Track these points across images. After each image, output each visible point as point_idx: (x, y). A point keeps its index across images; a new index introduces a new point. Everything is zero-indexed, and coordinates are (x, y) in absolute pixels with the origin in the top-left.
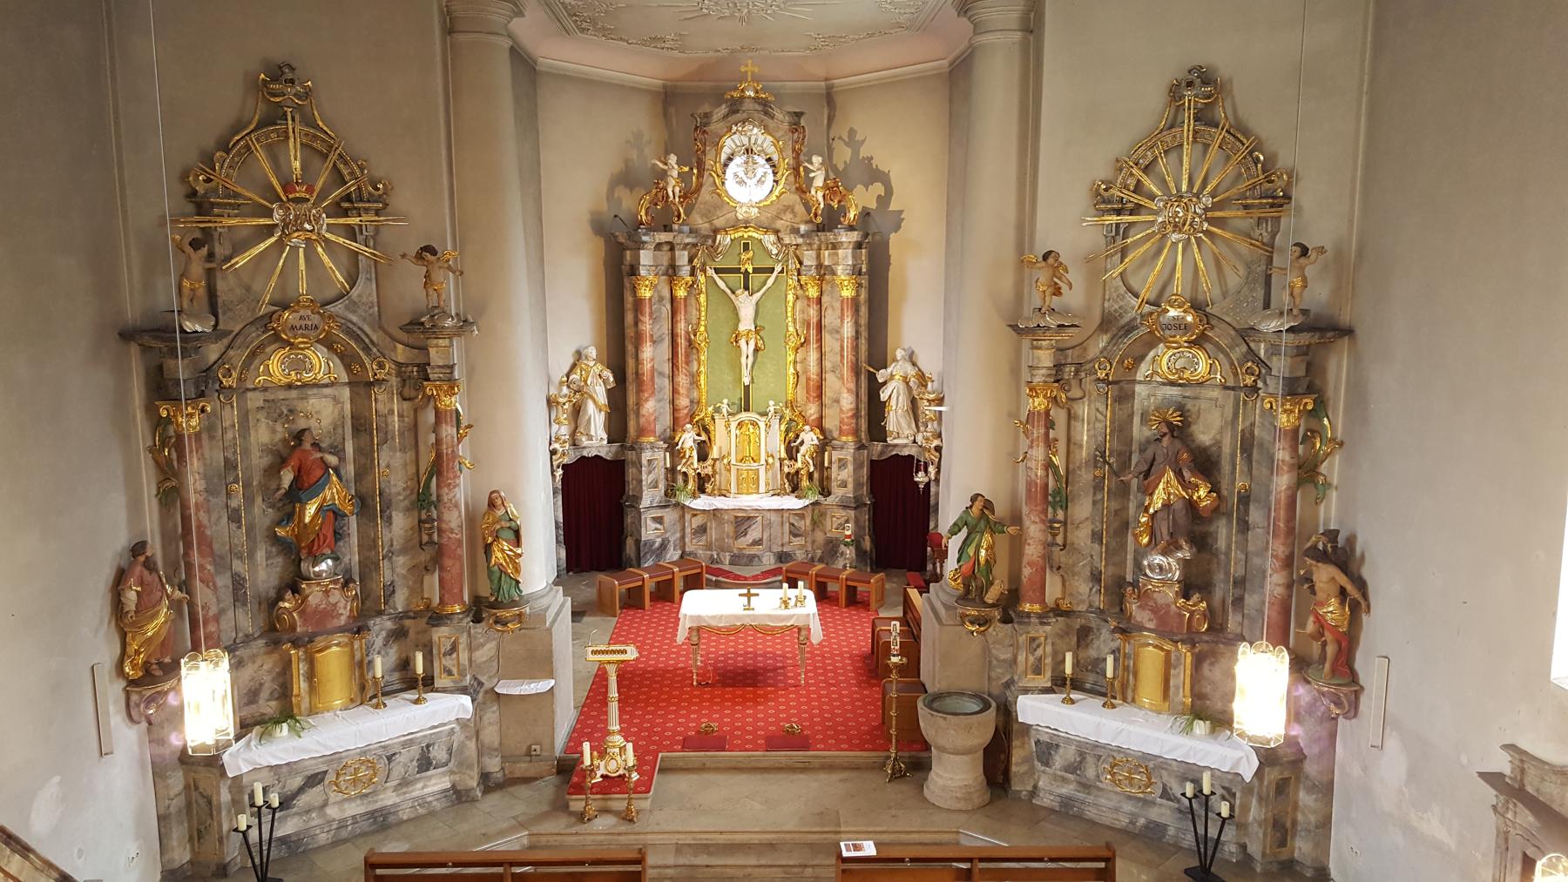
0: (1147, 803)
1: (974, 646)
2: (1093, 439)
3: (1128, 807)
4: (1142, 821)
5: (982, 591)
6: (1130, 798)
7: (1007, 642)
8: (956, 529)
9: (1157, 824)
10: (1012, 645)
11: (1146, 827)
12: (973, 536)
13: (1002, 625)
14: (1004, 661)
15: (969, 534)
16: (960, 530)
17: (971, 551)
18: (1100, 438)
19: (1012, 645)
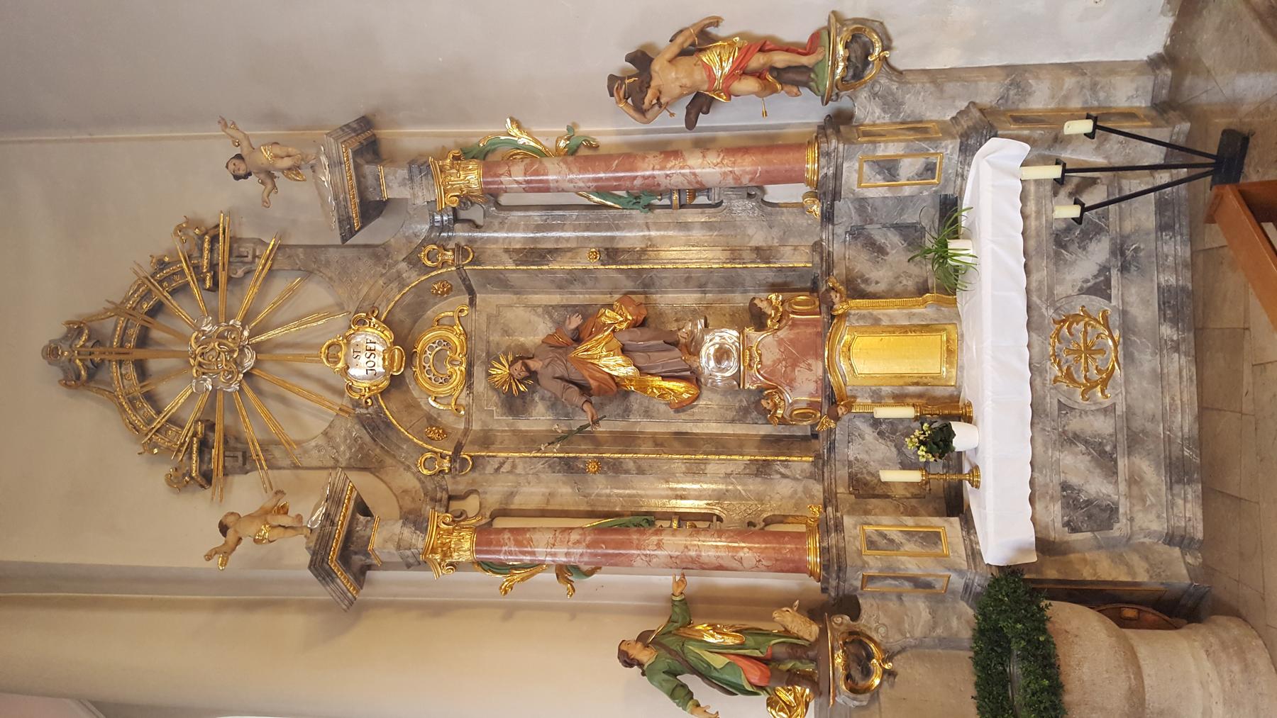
0: (1128, 328)
1: (912, 672)
2: (543, 476)
3: (1147, 360)
4: (1167, 331)
5: (798, 649)
6: (1129, 357)
7: (893, 605)
8: (682, 692)
9: (1163, 304)
10: (900, 597)
11: (1174, 322)
12: (692, 659)
13: (864, 616)
14: (933, 612)
15: (695, 671)
16: (684, 686)
17: (718, 661)
18: (540, 466)
19: (900, 597)
